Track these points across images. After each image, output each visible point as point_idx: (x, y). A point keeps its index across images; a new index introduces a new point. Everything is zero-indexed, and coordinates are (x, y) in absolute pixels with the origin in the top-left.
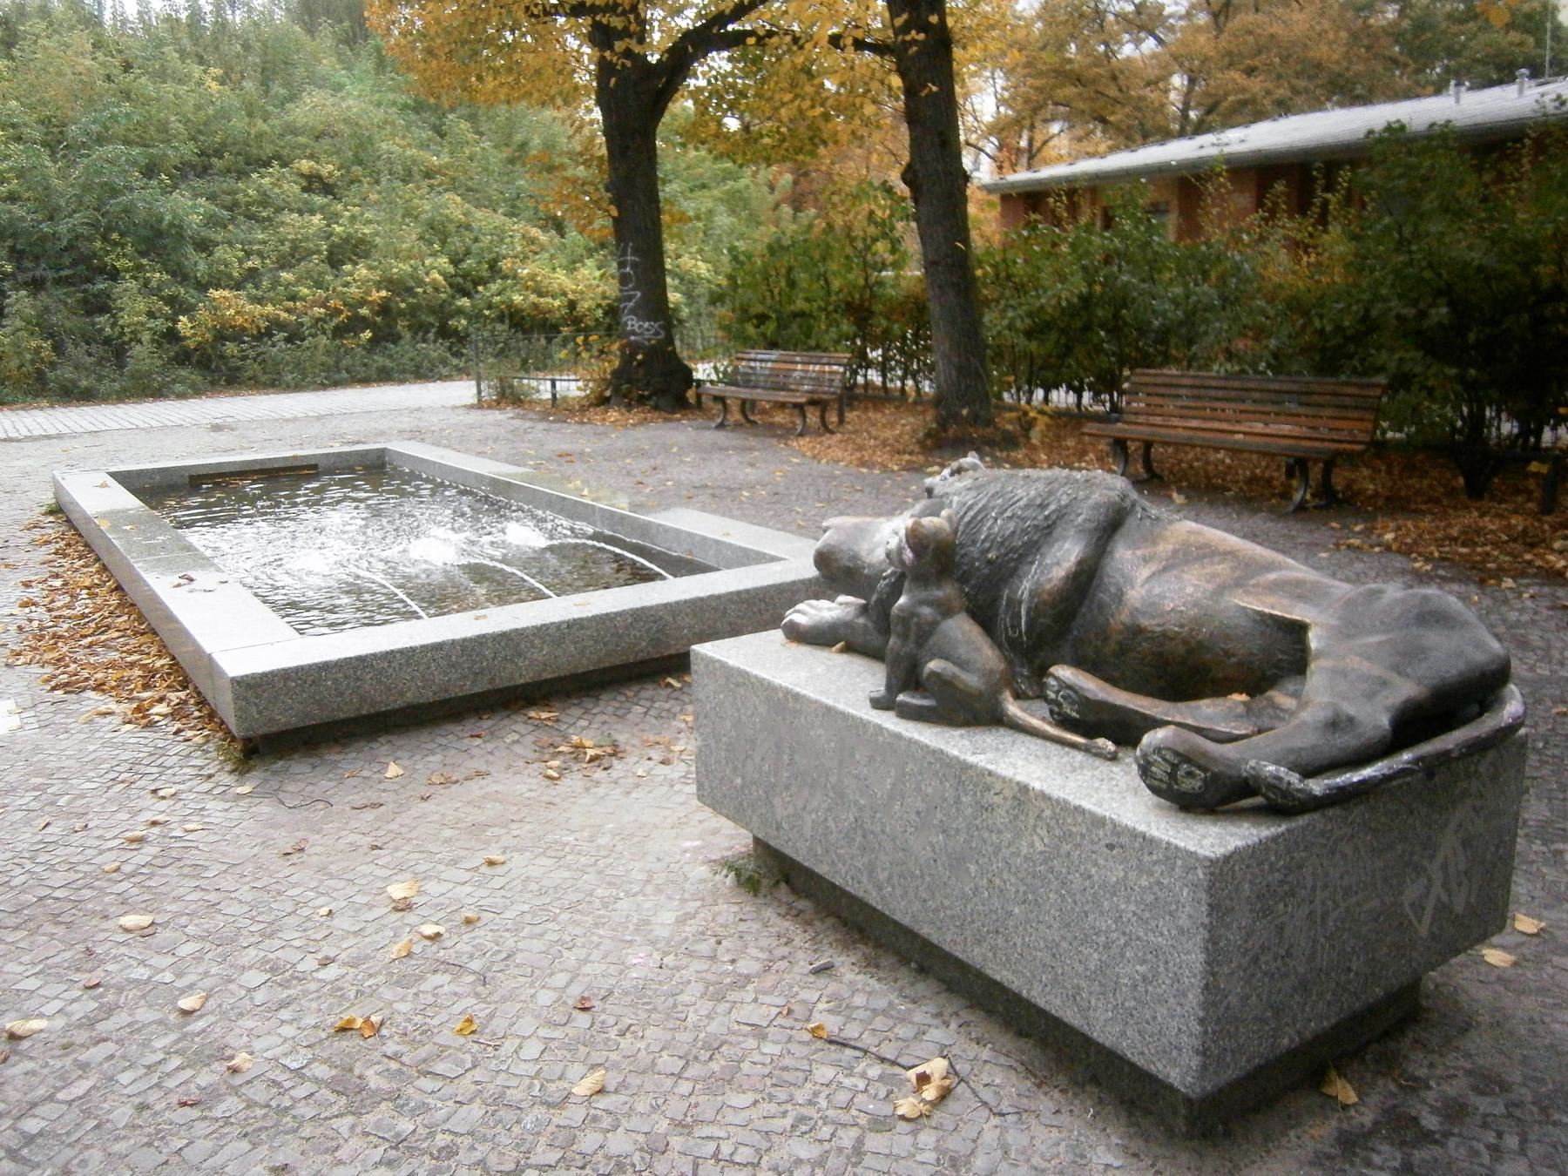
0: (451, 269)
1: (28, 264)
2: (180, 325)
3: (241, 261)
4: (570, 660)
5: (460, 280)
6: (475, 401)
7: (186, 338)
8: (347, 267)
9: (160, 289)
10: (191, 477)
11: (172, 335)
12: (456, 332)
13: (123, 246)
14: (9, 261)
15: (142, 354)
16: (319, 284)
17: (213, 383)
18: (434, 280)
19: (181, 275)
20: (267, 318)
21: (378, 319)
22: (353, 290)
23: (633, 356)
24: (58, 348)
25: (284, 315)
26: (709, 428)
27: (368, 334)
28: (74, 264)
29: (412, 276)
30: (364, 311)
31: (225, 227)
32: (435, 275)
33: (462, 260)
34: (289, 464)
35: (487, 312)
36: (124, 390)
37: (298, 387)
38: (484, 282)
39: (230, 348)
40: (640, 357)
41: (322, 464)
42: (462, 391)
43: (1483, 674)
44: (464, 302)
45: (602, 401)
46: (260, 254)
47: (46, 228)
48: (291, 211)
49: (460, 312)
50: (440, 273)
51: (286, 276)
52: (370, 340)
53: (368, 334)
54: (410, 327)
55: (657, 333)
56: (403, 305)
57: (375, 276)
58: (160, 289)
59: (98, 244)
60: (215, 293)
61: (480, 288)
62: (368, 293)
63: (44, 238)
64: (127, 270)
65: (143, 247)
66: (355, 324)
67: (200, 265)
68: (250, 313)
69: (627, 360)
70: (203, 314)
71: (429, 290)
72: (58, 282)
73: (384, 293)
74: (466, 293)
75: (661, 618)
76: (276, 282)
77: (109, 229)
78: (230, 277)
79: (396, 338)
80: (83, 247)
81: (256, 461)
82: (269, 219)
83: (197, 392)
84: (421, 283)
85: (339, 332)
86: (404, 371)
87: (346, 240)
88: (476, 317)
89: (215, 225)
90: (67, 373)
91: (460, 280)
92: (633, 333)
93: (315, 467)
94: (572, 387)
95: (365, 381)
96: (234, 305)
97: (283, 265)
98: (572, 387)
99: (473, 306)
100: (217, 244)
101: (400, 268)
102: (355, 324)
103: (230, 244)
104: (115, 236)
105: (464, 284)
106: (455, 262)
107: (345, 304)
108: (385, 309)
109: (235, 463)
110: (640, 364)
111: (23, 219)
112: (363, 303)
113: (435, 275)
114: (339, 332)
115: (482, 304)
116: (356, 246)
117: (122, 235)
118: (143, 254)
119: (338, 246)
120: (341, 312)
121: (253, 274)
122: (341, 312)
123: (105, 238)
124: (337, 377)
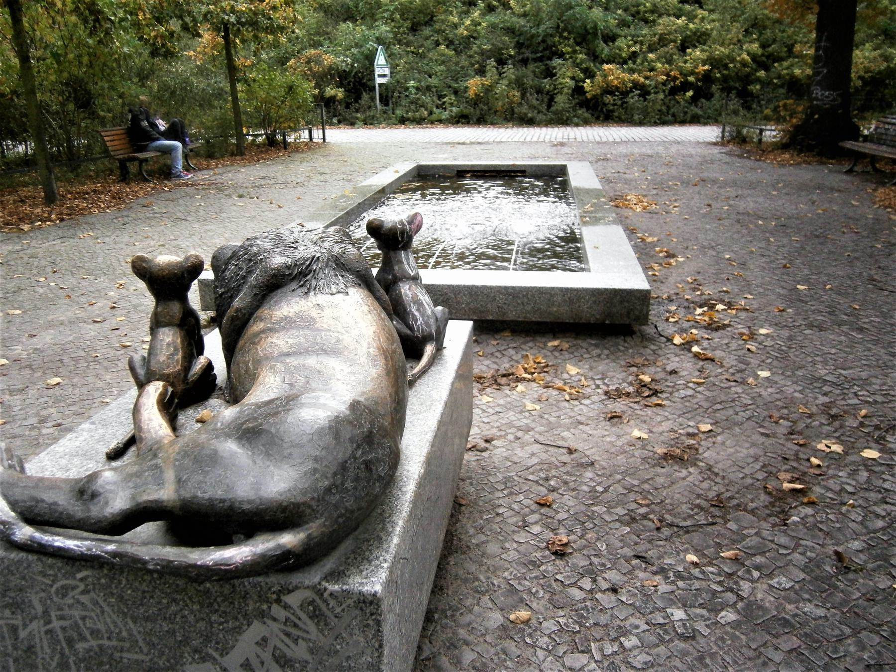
0: (760, 51)
1: (523, 50)
2: (585, 85)
3: (629, 47)
4: (564, 313)
5: (764, 59)
6: (719, 140)
7: (586, 92)
8: (688, 51)
9: (581, 63)
10: (458, 171)
11: (578, 90)
12: (751, 94)
13: (569, 39)
14: (514, 48)
15: (561, 101)
16: (670, 62)
17: (598, 118)
18: (743, 59)
19: (595, 56)
20: (633, 82)
21: (700, 84)
22: (688, 65)
23: (813, 114)
24: (523, 96)
25: (642, 80)
26: (839, 172)
27: (690, 93)
28: (545, 49)
29: (728, 56)
30: (691, 79)
31: (629, 27)
32: (745, 56)
33: (769, 46)
34: (509, 169)
35: (775, 81)
36: (552, 119)
37: (641, 124)
38: (780, 59)
39: (608, 99)
40: (816, 116)
41: (528, 170)
42: (710, 133)
43: (231, 508)
44: (762, 73)
45: (783, 147)
46: (642, 43)
47: (533, 31)
48: (669, 15)
49: (758, 80)
50: (748, 54)
51: (651, 56)
52: (692, 97)
53: (690, 93)
54: (722, 90)
55: (834, 100)
56: (718, 75)
57: (704, 56)
58: (581, 63)
59: (557, 39)
60: (606, 66)
61: (776, 65)
62: (696, 67)
63: (533, 36)
64: (568, 53)
65: (579, 40)
66: (686, 86)
67: (605, 50)
68: (623, 78)
69: (809, 117)
70: (599, 78)
71: (738, 65)
72: (535, 60)
73: (706, 67)
74: (767, 68)
75: (446, 294)
76: (645, 59)
77: (565, 29)
78: (620, 56)
79: (709, 96)
80: (549, 41)
81: (492, 166)
82: (654, 21)
83: (586, 123)
84: (733, 60)
85: (674, 91)
86: (709, 118)
87: (695, 33)
88: (765, 84)
89: (623, 26)
90: (524, 109)
91: (764, 59)
92: (817, 99)
93: (524, 172)
94: (771, 133)
95: (683, 122)
96: (615, 74)
97: (651, 49)
98: (771, 133)
99: (767, 76)
100: (621, 36)
101: (720, 51)
102: (686, 86)
103: (625, 37)
104: (565, 34)
105: (763, 62)
106: (763, 46)
107: (681, 74)
108: (707, 78)
109: (480, 165)
110: (817, 120)
111: (524, 26)
112: (692, 73)
113: (745, 56)
114: (674, 91)
115: (772, 75)
116: (700, 37)
117: (569, 33)
118: (578, 44)
119: (689, 37)
120: (678, 79)
121: (634, 55)
122: (678, 79)
123: (561, 36)
124: (667, 118)
